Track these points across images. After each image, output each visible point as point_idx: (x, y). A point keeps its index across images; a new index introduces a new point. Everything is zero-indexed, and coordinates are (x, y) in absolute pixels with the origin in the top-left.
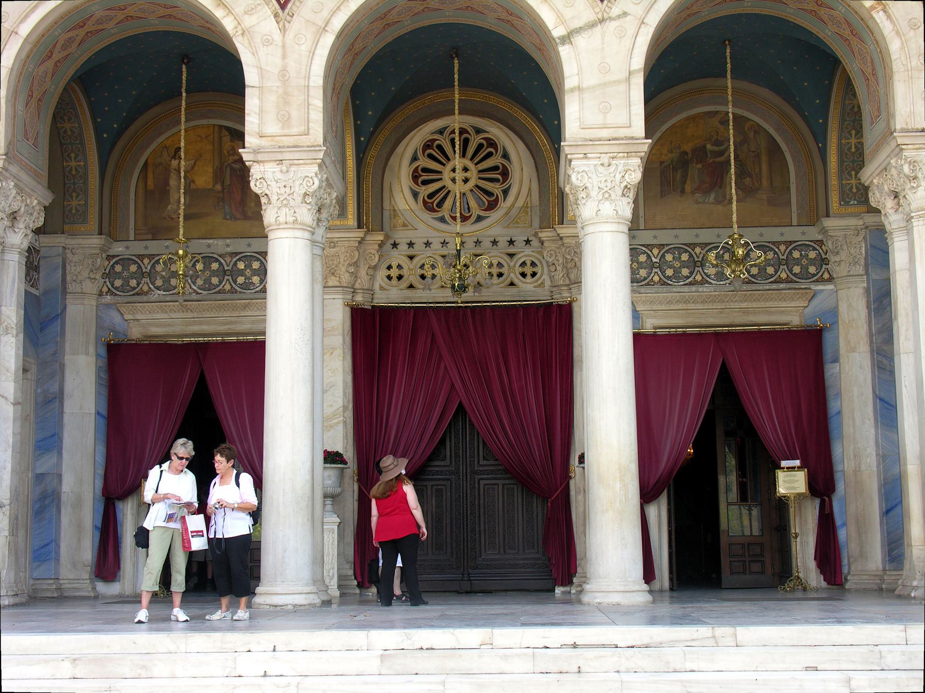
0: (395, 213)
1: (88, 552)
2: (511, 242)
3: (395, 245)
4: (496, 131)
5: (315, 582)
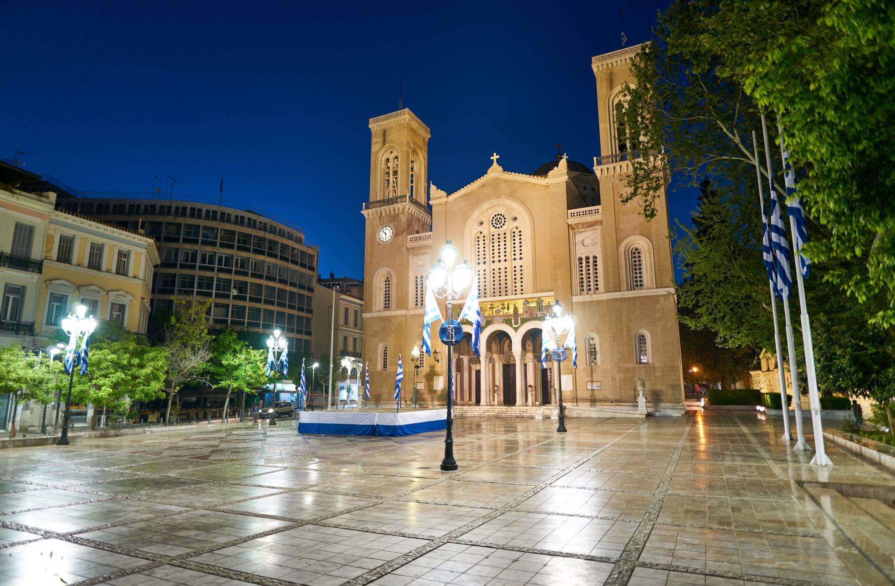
1: (468, 398)
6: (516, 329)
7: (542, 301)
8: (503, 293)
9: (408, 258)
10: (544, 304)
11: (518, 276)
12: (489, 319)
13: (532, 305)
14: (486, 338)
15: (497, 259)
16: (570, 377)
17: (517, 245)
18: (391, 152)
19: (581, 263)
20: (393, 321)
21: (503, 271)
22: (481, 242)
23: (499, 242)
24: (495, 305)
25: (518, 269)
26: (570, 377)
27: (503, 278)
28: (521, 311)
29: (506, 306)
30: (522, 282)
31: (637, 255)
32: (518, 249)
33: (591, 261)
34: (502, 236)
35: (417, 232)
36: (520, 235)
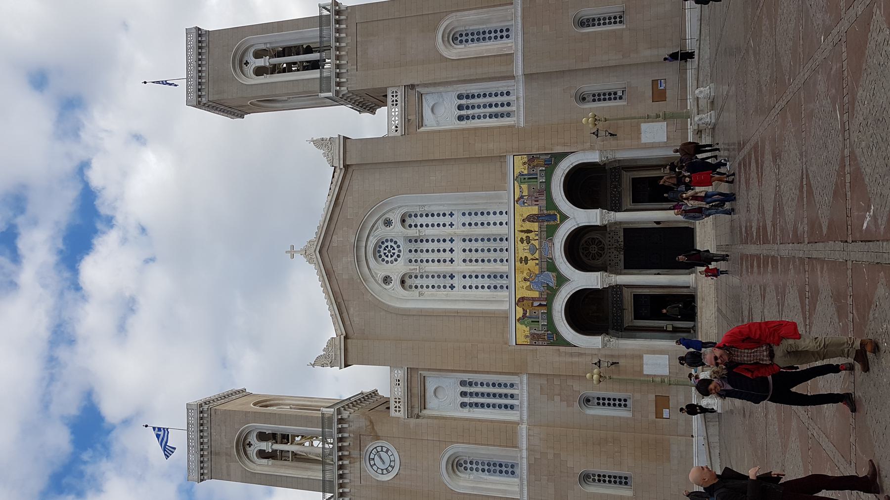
0: (602, 264)
2: (609, 237)
3: (610, 264)
4: (583, 241)
5: (690, 274)
6: (564, 218)
7: (521, 174)
8: (504, 245)
9: (429, 417)
10: (526, 172)
11: (479, 219)
12: (544, 265)
13: (525, 193)
14: (577, 271)
15: (448, 256)
16: (644, 126)
17: (430, 220)
18: (250, 445)
19: (468, 118)
20: (538, 456)
21: (468, 245)
22: (418, 282)
23: (422, 251)
24: (522, 254)
25: (467, 219)
26: (644, 126)
27: (479, 245)
28: (535, 210)
29: (524, 236)
30: (488, 213)
31: (464, 38)
32: (436, 220)
33: (464, 102)
34: (413, 246)
35: (388, 408)
36: (416, 216)
